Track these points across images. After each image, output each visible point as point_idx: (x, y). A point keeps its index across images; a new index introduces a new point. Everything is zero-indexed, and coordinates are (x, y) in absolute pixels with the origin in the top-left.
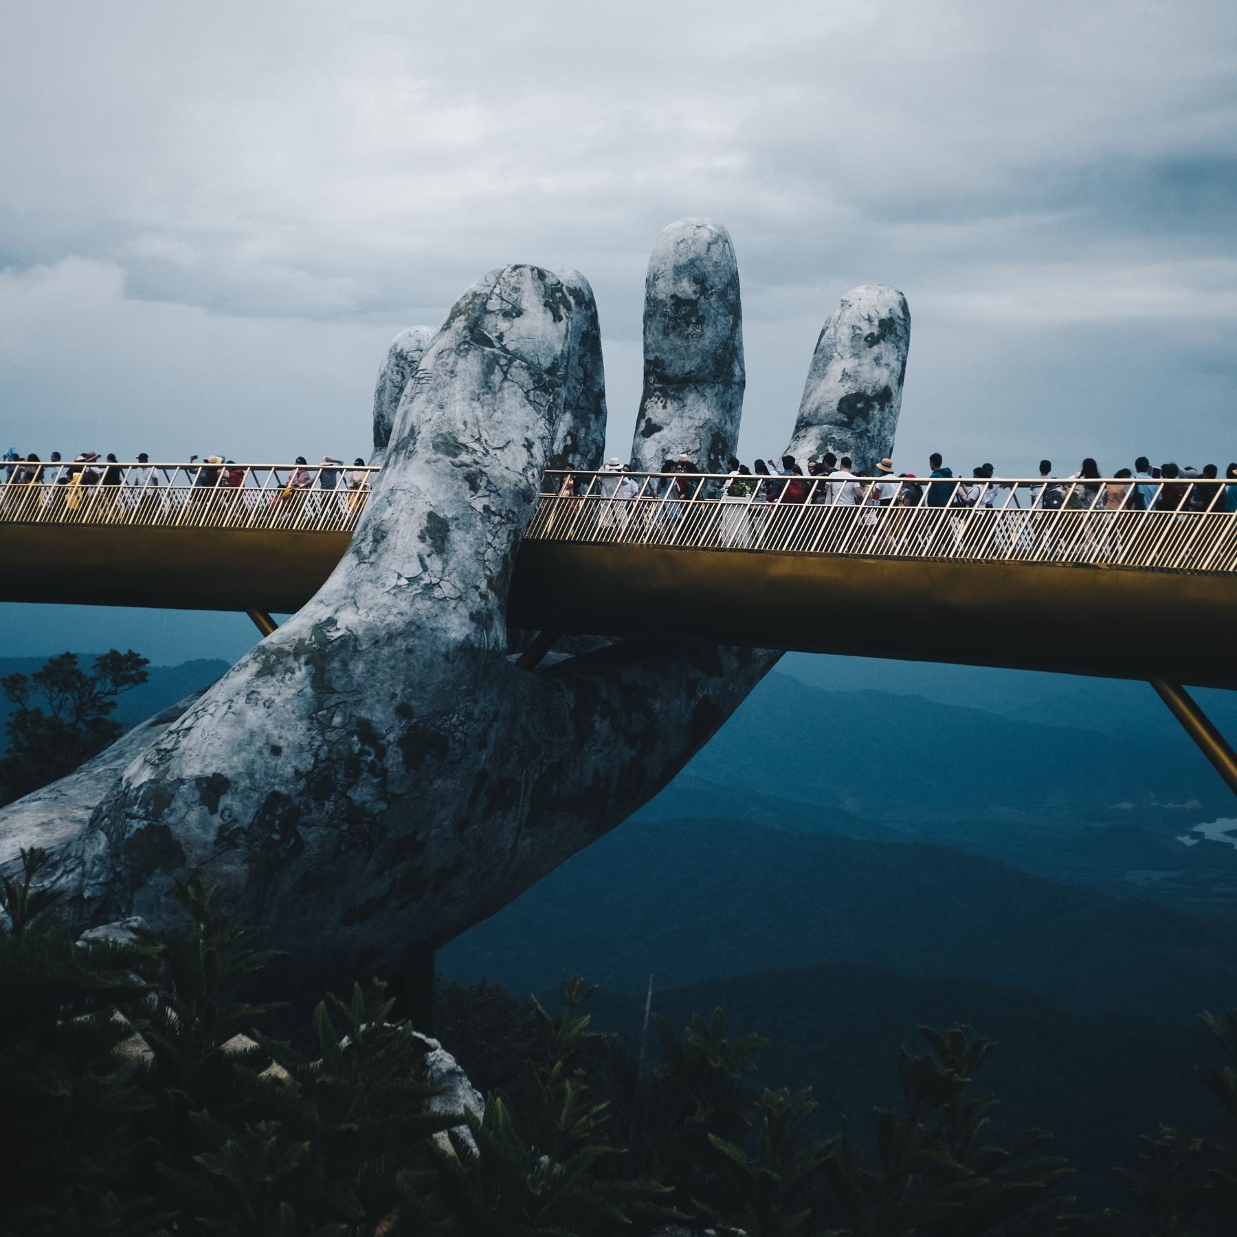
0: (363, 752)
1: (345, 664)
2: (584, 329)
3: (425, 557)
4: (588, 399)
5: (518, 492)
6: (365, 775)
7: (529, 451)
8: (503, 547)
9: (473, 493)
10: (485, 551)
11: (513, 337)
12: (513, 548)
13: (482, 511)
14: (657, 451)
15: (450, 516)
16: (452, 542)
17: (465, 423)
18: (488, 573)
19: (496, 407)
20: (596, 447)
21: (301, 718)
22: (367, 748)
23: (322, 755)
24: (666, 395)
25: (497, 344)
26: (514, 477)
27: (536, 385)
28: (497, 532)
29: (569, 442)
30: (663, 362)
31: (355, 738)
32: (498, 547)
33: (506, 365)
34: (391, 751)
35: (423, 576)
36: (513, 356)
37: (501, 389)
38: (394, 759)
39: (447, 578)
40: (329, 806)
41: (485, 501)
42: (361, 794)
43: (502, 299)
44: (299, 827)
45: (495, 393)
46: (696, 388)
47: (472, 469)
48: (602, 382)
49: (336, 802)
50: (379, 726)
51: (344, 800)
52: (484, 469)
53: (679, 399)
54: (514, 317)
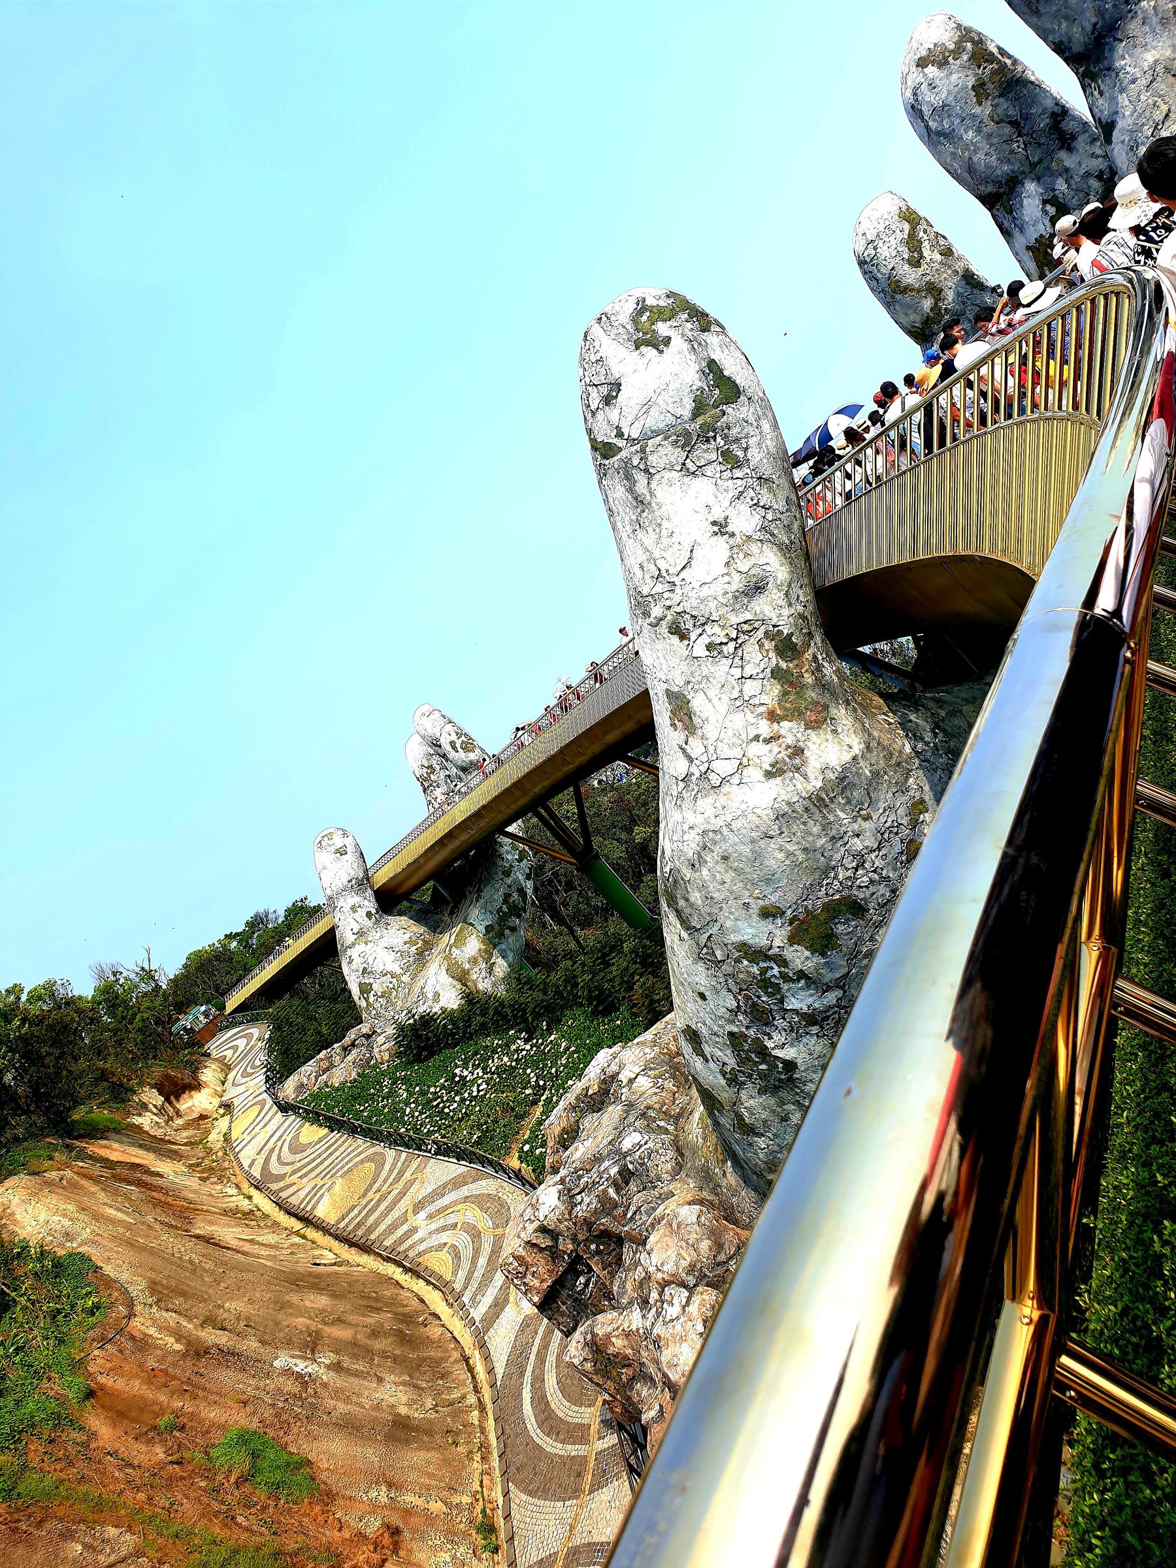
0: (764, 971)
1: (687, 900)
2: (971, 81)
3: (684, 746)
4: (1039, 145)
5: (736, 598)
6: (785, 987)
7: (723, 534)
8: (762, 666)
9: (686, 642)
10: (741, 691)
11: (631, 418)
12: (786, 647)
13: (708, 653)
14: (1127, 154)
15: (682, 684)
16: (698, 713)
17: (642, 567)
18: (762, 709)
19: (659, 522)
20: (1096, 177)
21: (695, 962)
22: (763, 965)
23: (735, 989)
24: (1094, 78)
25: (620, 443)
26: (717, 589)
27: (688, 449)
28: (742, 659)
29: (1052, 210)
30: (1061, 42)
31: (746, 963)
32: (754, 672)
33: (641, 459)
34: (789, 953)
35: (691, 770)
36: (641, 442)
37: (652, 494)
38: (800, 958)
39: (715, 756)
40: (779, 1022)
41: (705, 640)
42: (800, 1001)
43: (596, 386)
44: (774, 1053)
45: (650, 503)
46: (1115, 39)
47: (669, 617)
48: (1049, 103)
49: (784, 1018)
50: (757, 940)
51: (790, 1013)
52: (678, 609)
53: (1109, 69)
54: (616, 397)
